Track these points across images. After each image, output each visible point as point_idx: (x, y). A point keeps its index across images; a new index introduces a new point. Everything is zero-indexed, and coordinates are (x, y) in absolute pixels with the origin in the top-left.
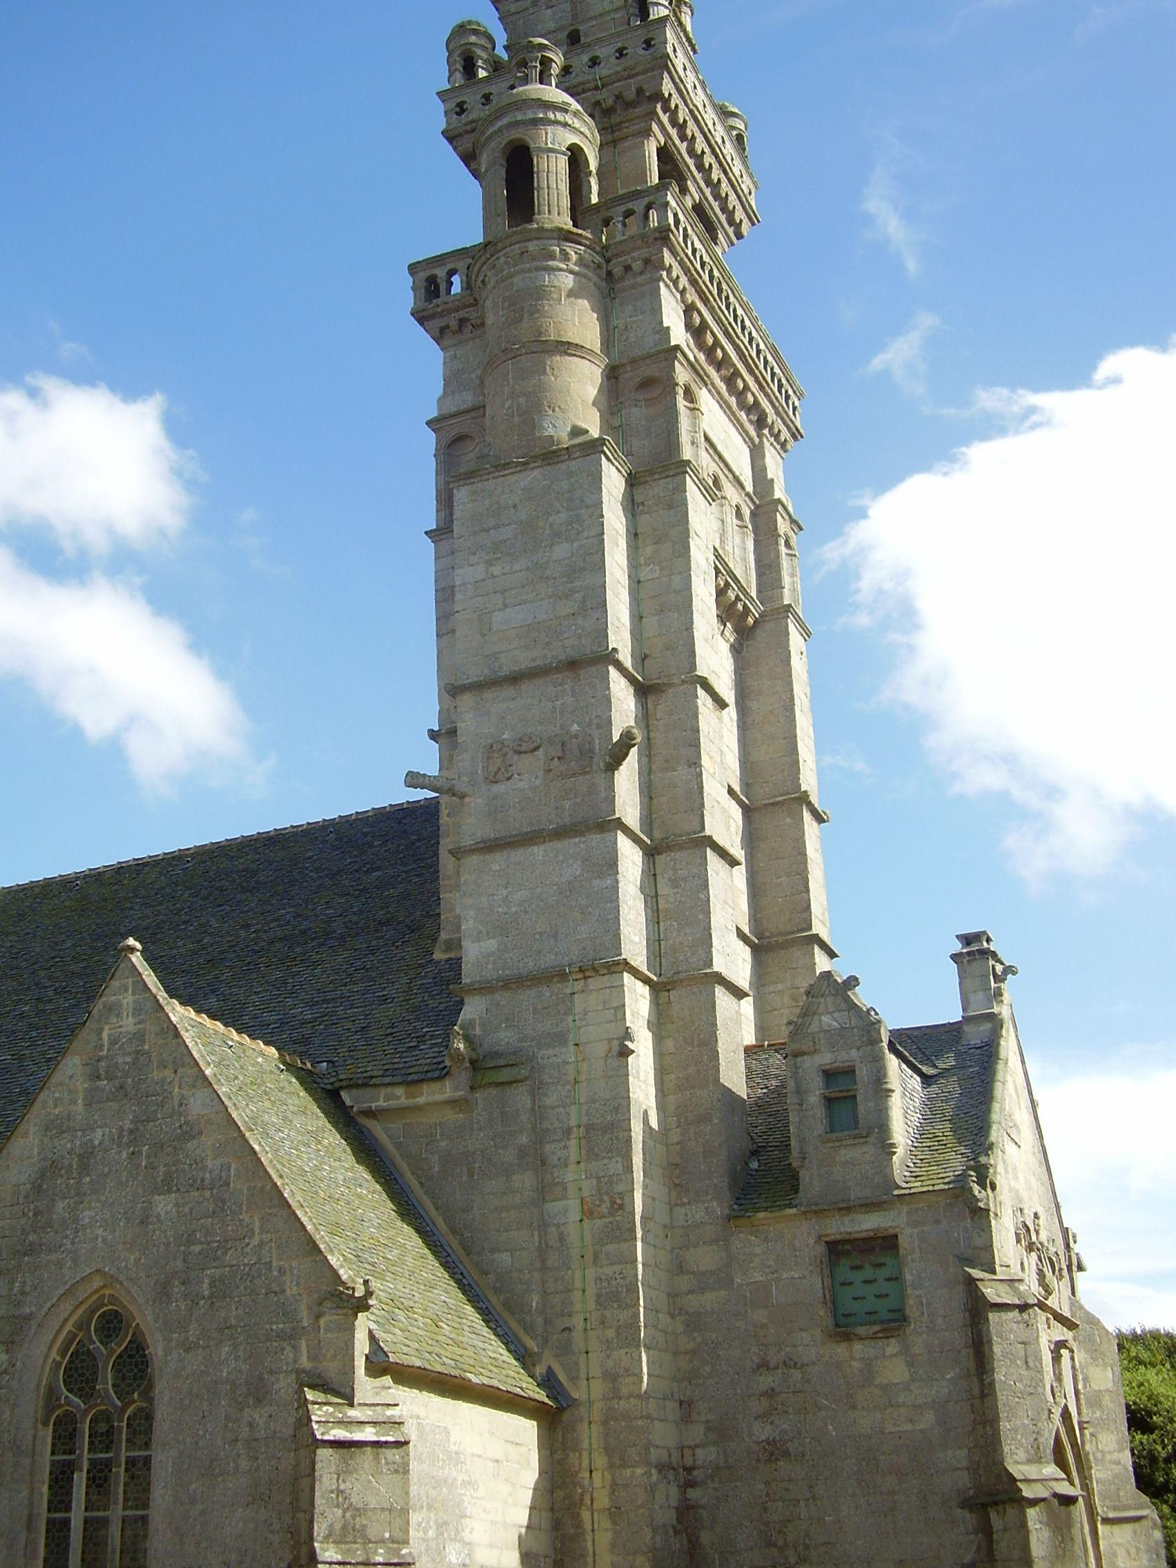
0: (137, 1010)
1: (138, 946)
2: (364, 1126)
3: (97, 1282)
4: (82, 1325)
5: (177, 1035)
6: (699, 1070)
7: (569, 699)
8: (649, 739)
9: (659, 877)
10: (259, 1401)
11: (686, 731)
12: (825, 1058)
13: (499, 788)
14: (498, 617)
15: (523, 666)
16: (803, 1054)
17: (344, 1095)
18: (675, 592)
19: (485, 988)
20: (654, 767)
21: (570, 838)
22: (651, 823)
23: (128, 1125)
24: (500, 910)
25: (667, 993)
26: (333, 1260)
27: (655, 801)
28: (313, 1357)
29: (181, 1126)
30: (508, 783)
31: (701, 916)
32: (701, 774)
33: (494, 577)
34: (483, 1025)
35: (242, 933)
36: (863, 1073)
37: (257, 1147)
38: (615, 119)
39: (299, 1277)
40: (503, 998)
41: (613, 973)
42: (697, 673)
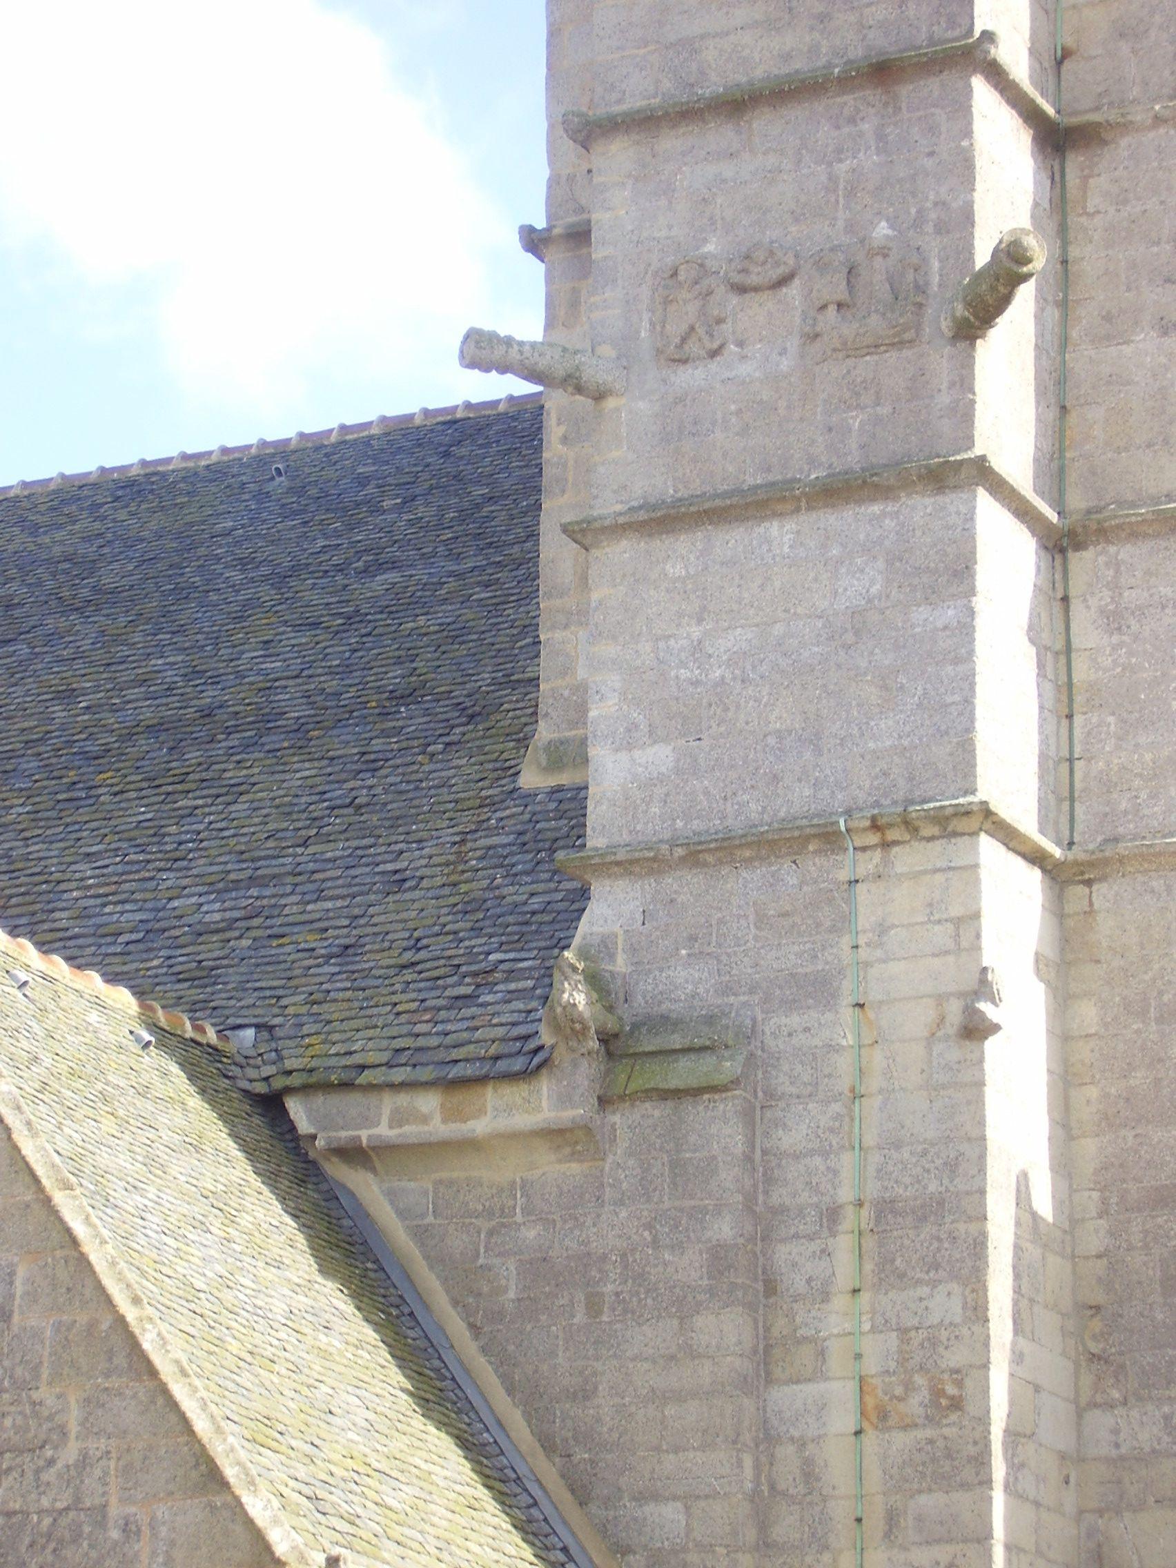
2: (344, 1187)
6: (1157, 1081)
7: (870, 160)
8: (1064, 262)
9: (1076, 606)
11: (1158, 243)
13: (689, 378)
15: (759, 73)
17: (296, 1108)
20: (1074, 334)
21: (860, 502)
22: (1062, 470)
25: (1082, 890)
26: (257, 1507)
27: (1073, 419)
30: (714, 366)
34: (633, 950)
35: (59, 712)
37: (79, 1229)
39: (172, 1543)
41: (955, 834)
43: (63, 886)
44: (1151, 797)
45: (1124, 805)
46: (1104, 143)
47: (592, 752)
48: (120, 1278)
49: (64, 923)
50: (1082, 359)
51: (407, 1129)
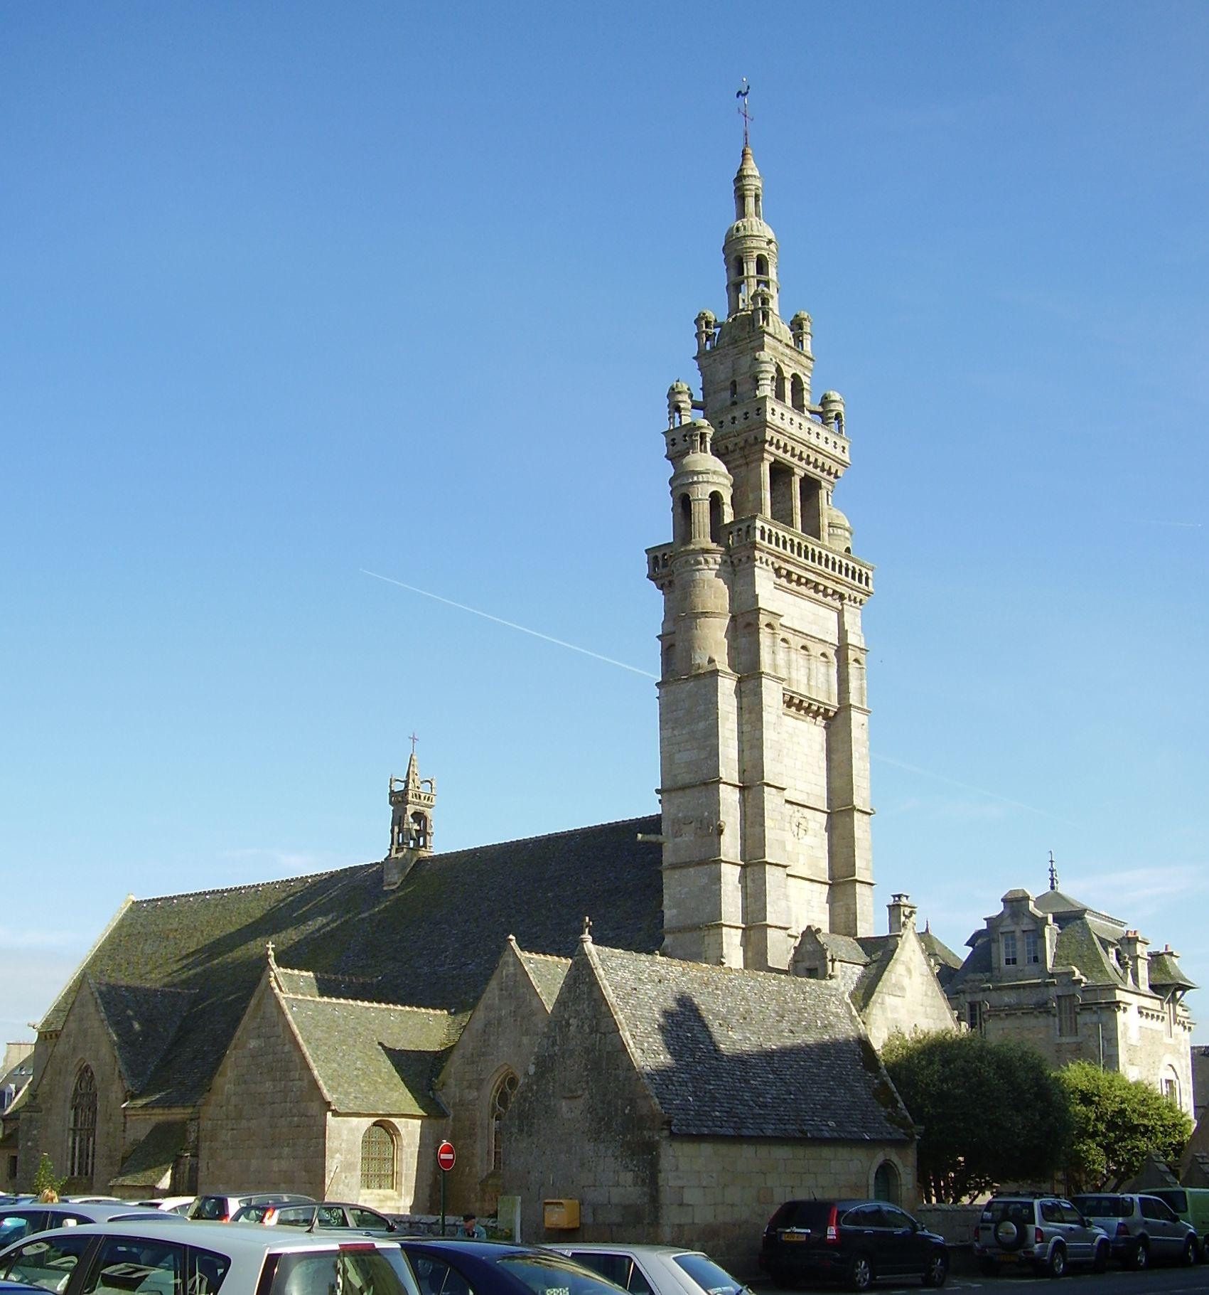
0: (514, 965)
1: (513, 938)
3: (506, 1067)
4: (503, 1082)
13: (677, 840)
14: (677, 756)
16: (798, 962)
19: (671, 931)
23: (513, 1009)
32: (764, 831)
33: (675, 736)
38: (746, 452)
40: (679, 935)
42: (765, 781)
50: (748, 830)
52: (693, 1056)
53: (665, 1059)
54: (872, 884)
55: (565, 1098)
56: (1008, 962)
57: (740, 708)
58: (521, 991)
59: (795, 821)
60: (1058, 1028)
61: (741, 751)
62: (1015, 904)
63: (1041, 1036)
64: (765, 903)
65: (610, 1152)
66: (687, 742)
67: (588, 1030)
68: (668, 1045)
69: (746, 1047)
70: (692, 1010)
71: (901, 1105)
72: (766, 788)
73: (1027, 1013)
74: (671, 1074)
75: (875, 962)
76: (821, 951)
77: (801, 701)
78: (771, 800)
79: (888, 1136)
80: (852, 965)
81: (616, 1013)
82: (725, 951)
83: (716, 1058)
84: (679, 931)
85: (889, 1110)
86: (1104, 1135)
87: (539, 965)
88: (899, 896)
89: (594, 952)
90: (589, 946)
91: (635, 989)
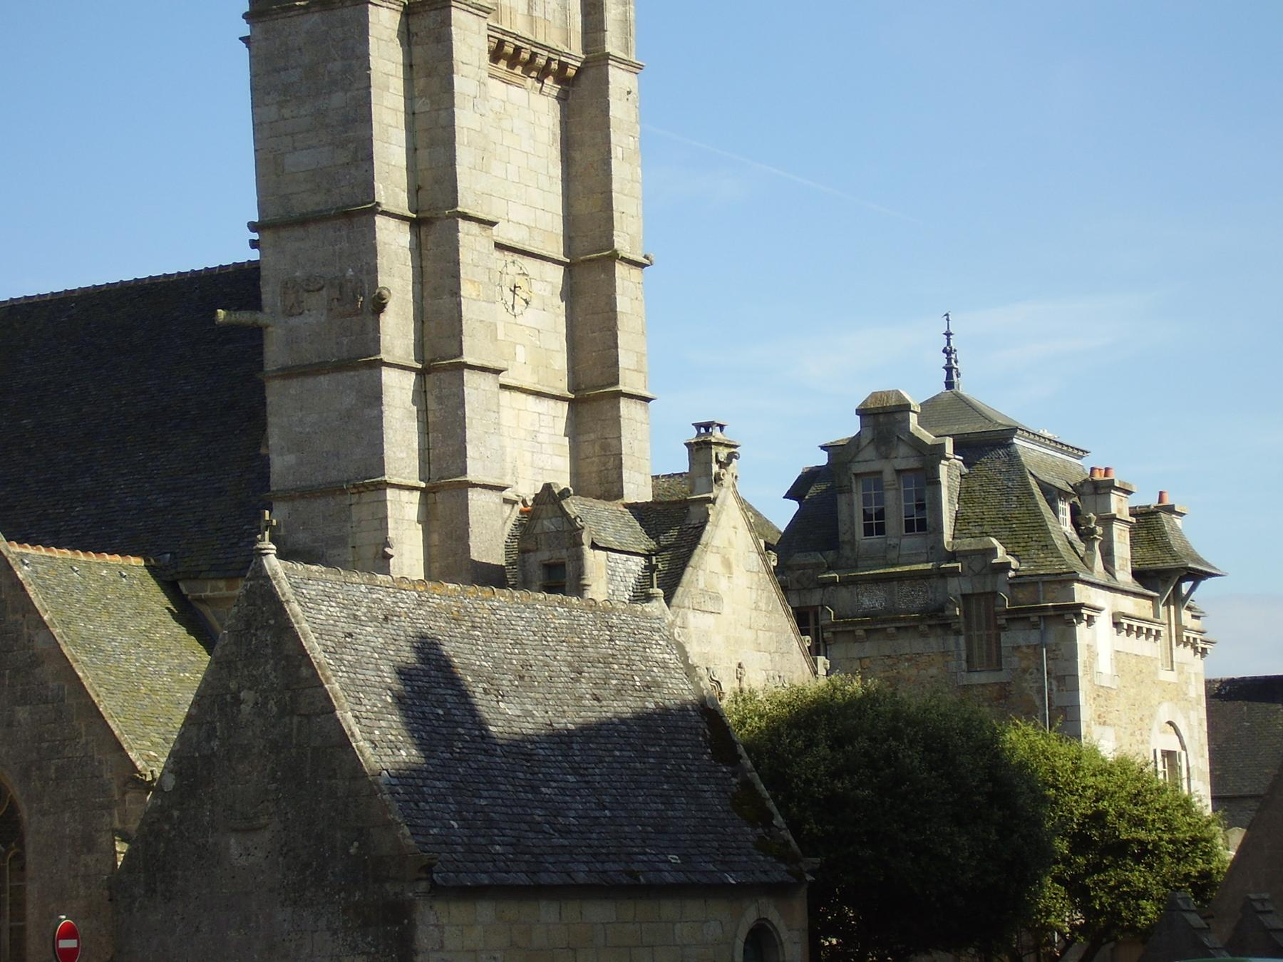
5: (23, 589)
6: (456, 562)
7: (345, 245)
8: (421, 267)
10: (90, 851)
11: (449, 262)
12: (544, 556)
13: (294, 321)
15: (309, 209)
16: (529, 551)
17: (182, 586)
18: (442, 127)
19: (289, 496)
20: (425, 294)
21: (347, 371)
22: (423, 345)
24: (297, 429)
25: (432, 495)
26: (133, 755)
27: (425, 325)
28: (123, 821)
29: (30, 657)
30: (301, 318)
31: (459, 430)
32: (459, 304)
36: (570, 568)
37: (80, 674)
42: (459, 209)
43: (114, 488)
44: (453, 462)
45: (444, 466)
46: (432, 223)
47: (270, 456)
48: (93, 689)
49: (113, 505)
51: (216, 593)
52: (449, 747)
53: (408, 754)
54: (647, 400)
55: (235, 830)
56: (868, 531)
57: (409, 66)
58: (11, 618)
59: (508, 282)
60: (964, 657)
61: (412, 150)
62: (881, 419)
63: (933, 671)
64: (464, 441)
65: (322, 923)
66: (308, 131)
67: (275, 709)
68: (412, 732)
69: (528, 728)
70: (439, 668)
71: (779, 820)
72: (463, 225)
73: (906, 628)
74: (420, 782)
75: (665, 548)
76: (571, 535)
77: (534, 55)
78: (471, 242)
79: (764, 878)
80: (624, 557)
81: (328, 679)
82: (391, 534)
83: (486, 751)
84: (302, 496)
85: (760, 830)
86: (1066, 861)
87: (39, 568)
88: (708, 426)
89: (281, 574)
90: (273, 564)
91: (350, 635)
